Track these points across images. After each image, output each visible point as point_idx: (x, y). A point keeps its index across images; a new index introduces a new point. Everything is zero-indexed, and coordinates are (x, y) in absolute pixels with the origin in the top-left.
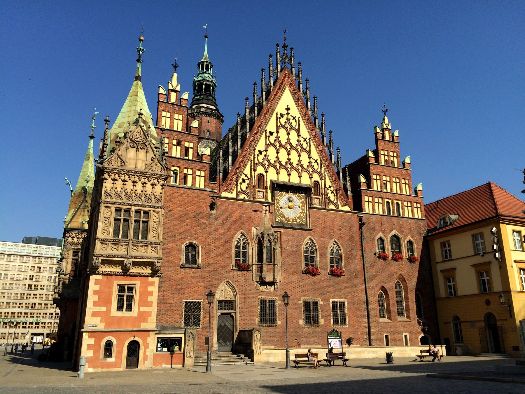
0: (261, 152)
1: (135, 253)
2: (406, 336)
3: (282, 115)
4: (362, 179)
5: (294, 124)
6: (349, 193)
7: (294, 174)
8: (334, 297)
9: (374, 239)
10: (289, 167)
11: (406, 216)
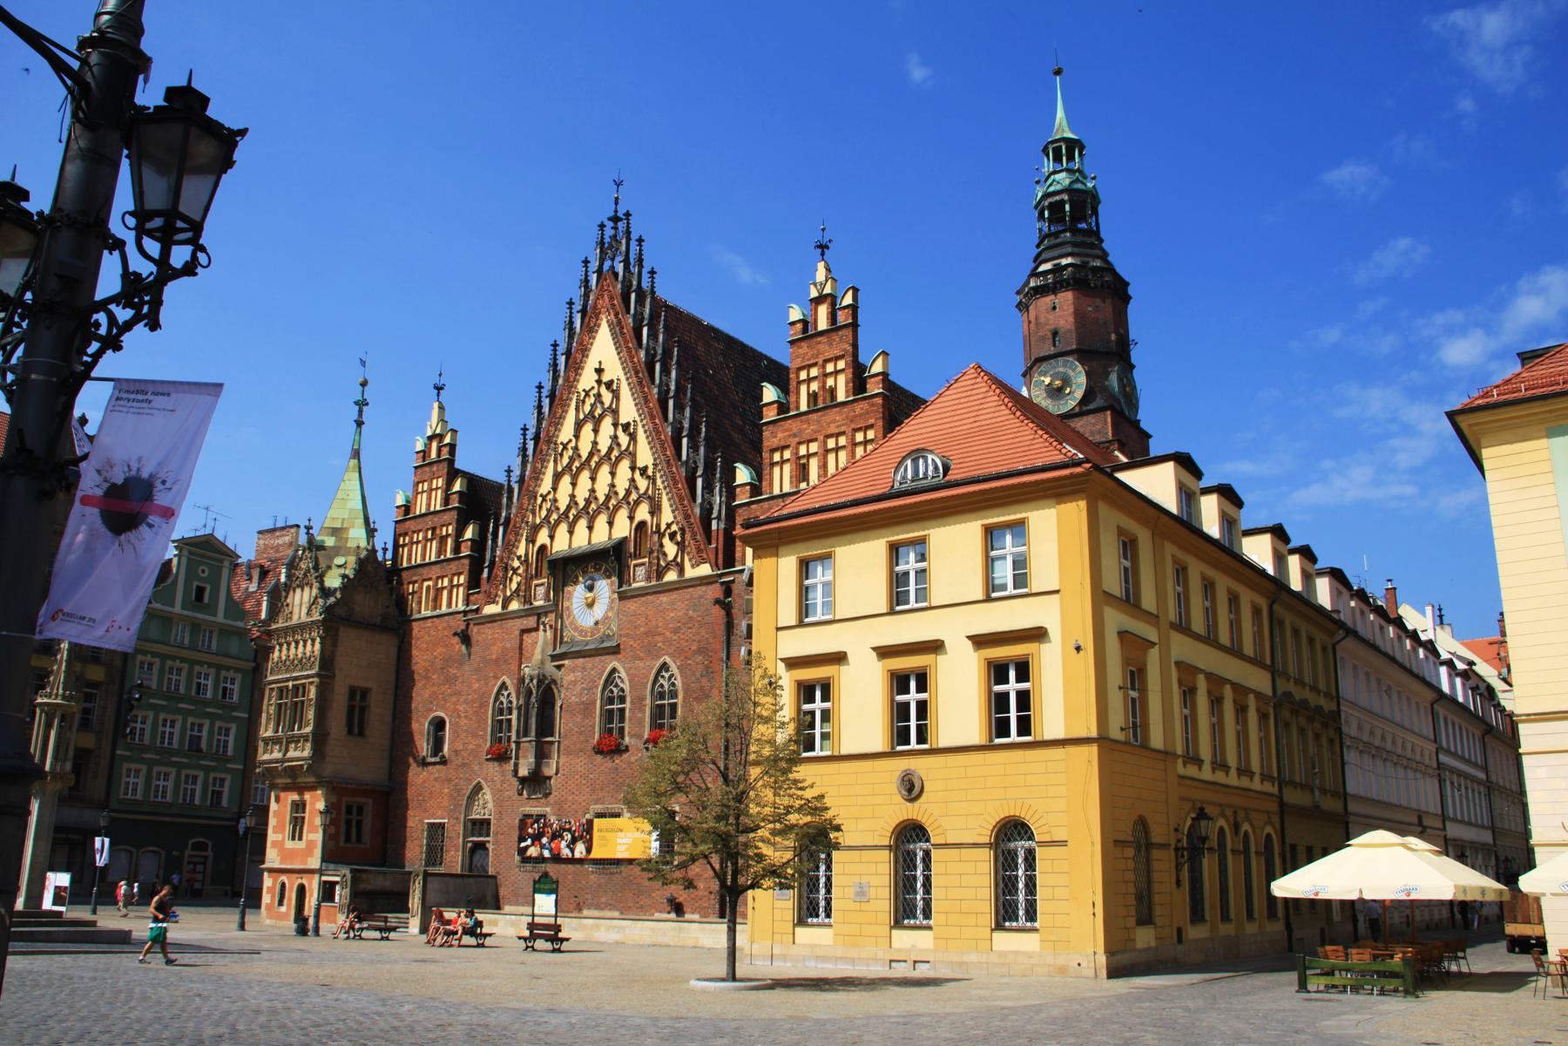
0: (544, 498)
1: (291, 754)
7: (602, 520)
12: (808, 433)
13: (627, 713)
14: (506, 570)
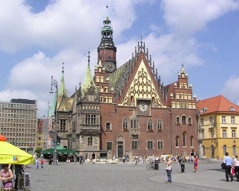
0: (132, 88)
1: (92, 128)
2: (185, 153)
3: (140, 72)
4: (172, 95)
5: (145, 76)
6: (166, 101)
7: (145, 95)
8: (159, 140)
9: (175, 118)
10: (143, 92)
11: (189, 108)
12: (182, 91)
13: (153, 127)
14: (124, 98)
